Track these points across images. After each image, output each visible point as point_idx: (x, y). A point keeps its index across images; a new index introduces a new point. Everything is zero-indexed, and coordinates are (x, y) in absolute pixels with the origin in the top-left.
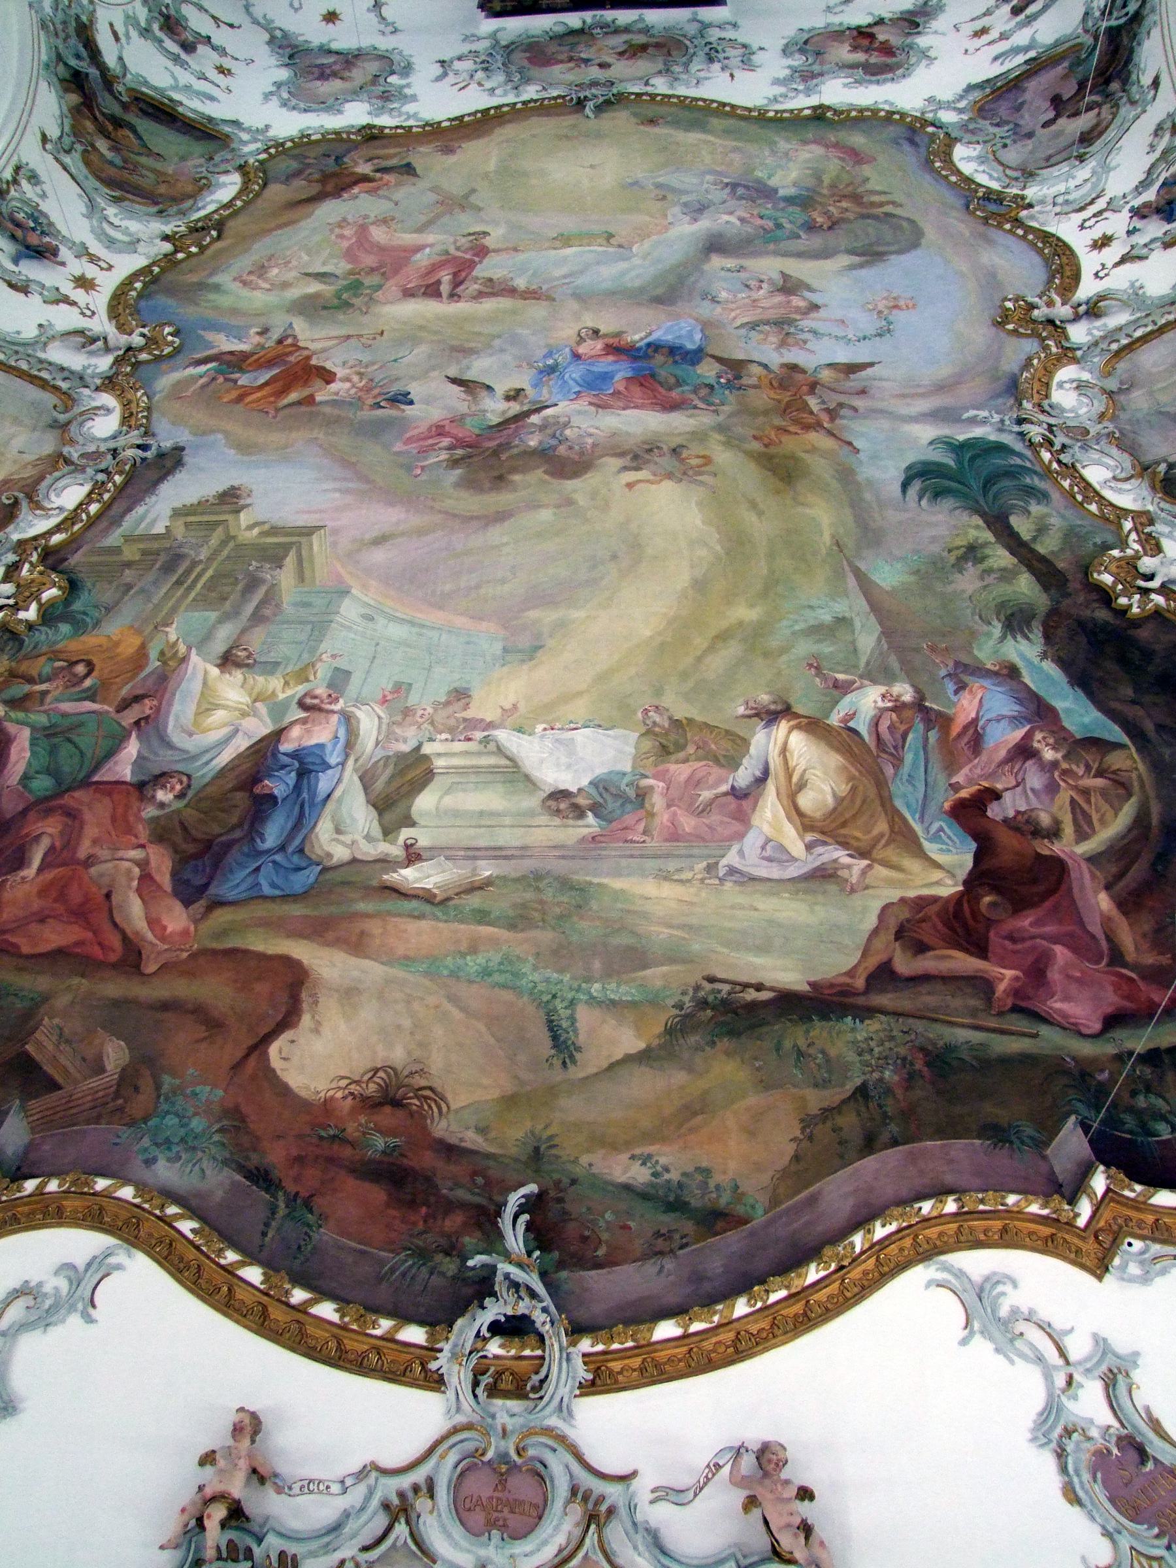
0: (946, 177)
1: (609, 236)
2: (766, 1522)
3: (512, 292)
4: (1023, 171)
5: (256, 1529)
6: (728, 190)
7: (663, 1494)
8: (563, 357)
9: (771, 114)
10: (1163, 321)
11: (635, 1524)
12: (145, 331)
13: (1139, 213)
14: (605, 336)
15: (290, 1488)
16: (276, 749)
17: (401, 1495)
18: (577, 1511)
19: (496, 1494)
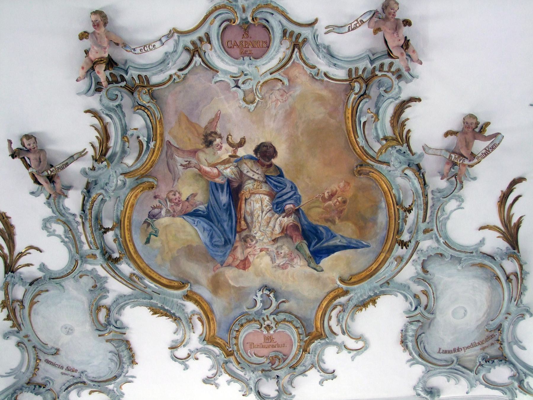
2: (386, 42)
5: (123, 67)
7: (332, 29)
11: (317, 45)
15: (134, 50)
17: (193, 43)
18: (287, 44)
19: (244, 40)
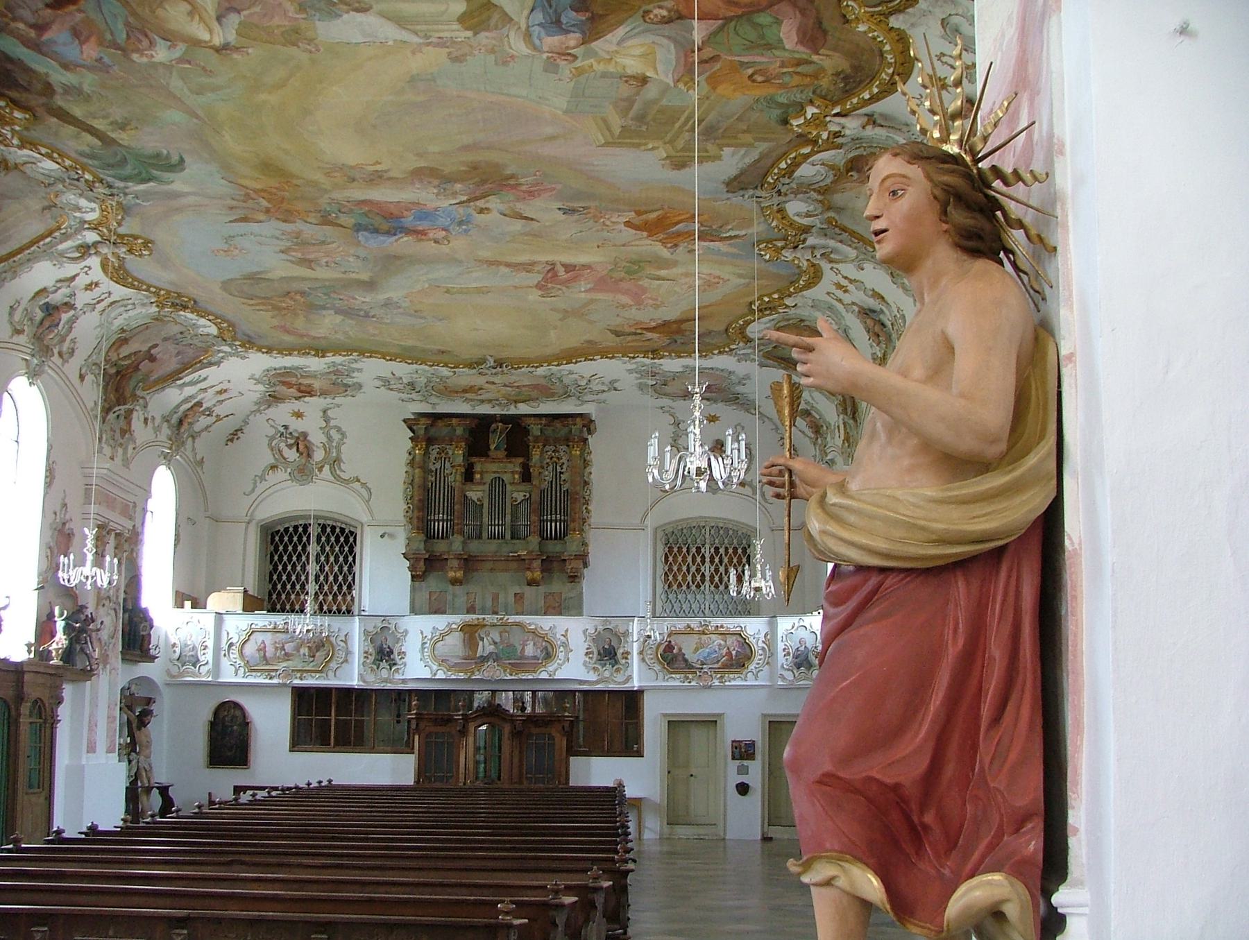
0: (217, 318)
1: (448, 291)
3: (508, 265)
4: (162, 320)
6: (371, 314)
8: (455, 229)
9: (355, 354)
10: (32, 249)
12: (783, 258)
13: (69, 306)
14: (430, 240)
16: (583, 33)
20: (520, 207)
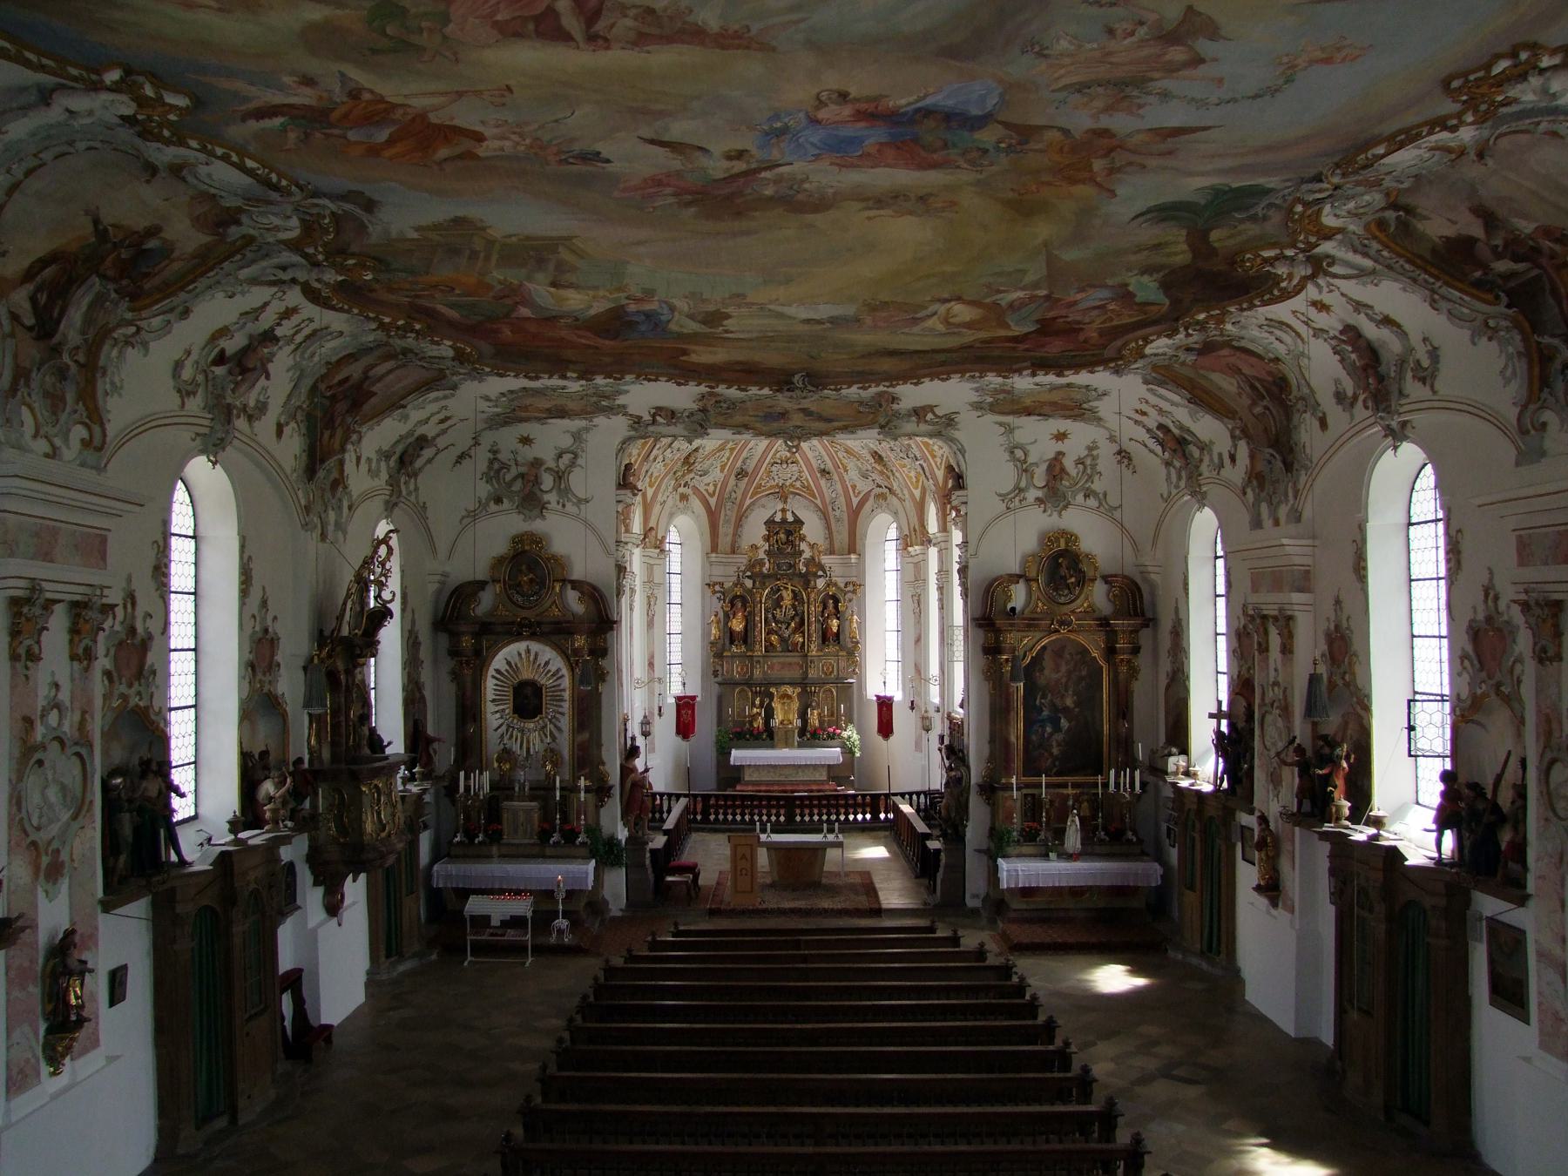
3: (697, 35)
14: (857, 100)
20: (675, 163)
